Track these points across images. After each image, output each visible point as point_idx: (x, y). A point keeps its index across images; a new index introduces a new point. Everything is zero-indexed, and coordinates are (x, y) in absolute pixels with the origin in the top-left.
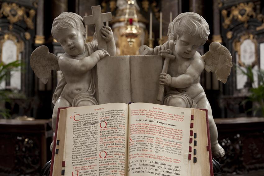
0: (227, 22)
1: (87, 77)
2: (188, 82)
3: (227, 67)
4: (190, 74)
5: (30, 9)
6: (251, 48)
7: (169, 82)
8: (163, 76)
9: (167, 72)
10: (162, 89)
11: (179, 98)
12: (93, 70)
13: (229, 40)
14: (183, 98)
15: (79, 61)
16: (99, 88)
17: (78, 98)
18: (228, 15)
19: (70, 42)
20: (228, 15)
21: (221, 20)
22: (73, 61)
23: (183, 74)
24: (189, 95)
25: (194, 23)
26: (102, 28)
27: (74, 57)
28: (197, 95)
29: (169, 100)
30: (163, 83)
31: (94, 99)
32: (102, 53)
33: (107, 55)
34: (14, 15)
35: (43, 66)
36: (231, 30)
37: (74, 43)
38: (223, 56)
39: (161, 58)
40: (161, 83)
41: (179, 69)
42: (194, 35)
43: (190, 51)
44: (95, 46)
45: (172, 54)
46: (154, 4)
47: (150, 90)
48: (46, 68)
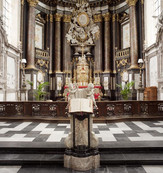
0: (118, 65)
5: (47, 61)
6: (127, 75)
13: (119, 72)
18: (119, 63)
20: (119, 63)
21: (116, 65)
34: (42, 64)
36: (120, 68)
46: (92, 59)
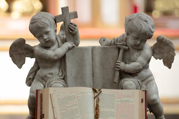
1: (58, 64)
2: (138, 68)
3: (171, 56)
4: (140, 62)
7: (122, 68)
8: (118, 63)
9: (121, 60)
10: (117, 74)
11: (129, 82)
12: (62, 59)
14: (134, 81)
15: (52, 51)
16: (67, 72)
17: (51, 80)
19: (46, 37)
22: (47, 51)
23: (135, 61)
24: (139, 78)
25: (141, 24)
26: (70, 24)
27: (47, 48)
28: (146, 79)
29: (123, 82)
30: (119, 69)
31: (64, 81)
32: (69, 44)
33: (74, 47)
35: (19, 54)
37: (49, 38)
38: (168, 46)
39: (117, 49)
40: (117, 69)
41: (132, 58)
42: (141, 33)
43: (139, 44)
44: (63, 38)
45: (126, 45)
47: (108, 74)
48: (22, 56)
